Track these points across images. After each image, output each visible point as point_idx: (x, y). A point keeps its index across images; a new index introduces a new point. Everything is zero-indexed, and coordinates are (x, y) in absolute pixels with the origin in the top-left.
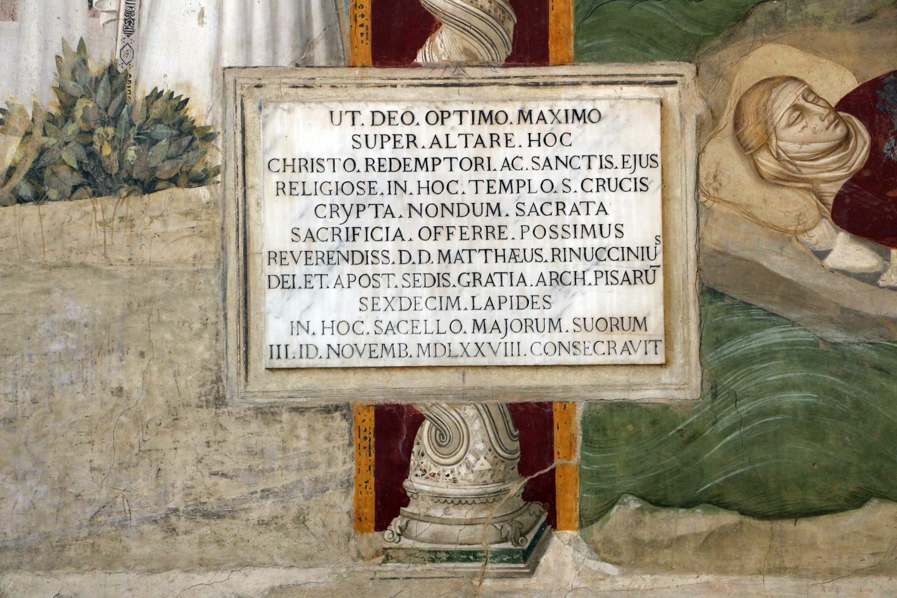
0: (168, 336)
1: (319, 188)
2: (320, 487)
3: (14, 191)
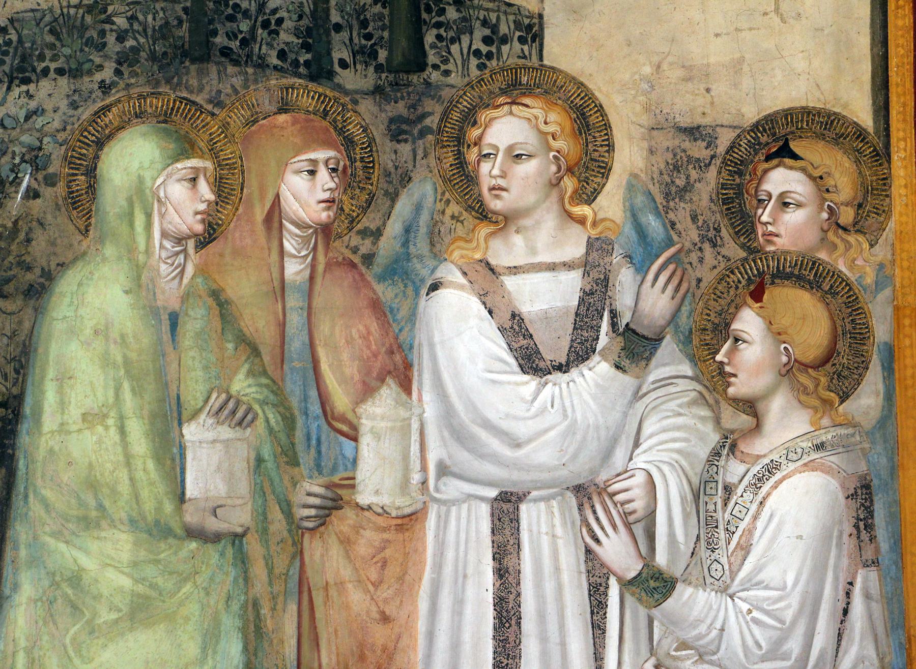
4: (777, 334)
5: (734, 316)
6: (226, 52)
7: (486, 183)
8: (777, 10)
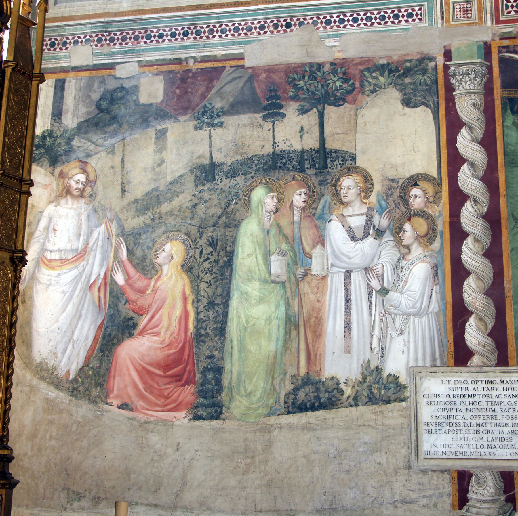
0: (394, 447)
1: (439, 403)
2: (441, 495)
3: (349, 403)
4: (414, 229)
5: (403, 225)
6: (280, 167)
7: (342, 195)
8: (413, 150)
